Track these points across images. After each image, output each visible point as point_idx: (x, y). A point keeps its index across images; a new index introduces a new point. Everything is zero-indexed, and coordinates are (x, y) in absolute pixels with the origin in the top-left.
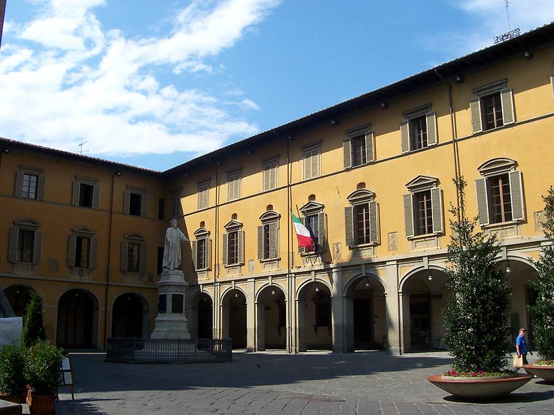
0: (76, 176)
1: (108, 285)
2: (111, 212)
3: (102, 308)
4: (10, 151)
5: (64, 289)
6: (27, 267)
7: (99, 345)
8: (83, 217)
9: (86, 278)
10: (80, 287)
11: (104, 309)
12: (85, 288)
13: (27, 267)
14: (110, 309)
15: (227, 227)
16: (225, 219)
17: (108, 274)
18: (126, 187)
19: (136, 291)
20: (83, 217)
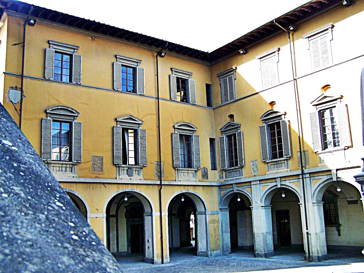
0: (116, 56)
1: (161, 185)
2: (158, 98)
3: (156, 214)
4: (35, 21)
5: (113, 192)
6: (66, 168)
7: (155, 258)
8: (127, 105)
9: (136, 179)
10: (129, 189)
11: (159, 214)
13: (66, 168)
14: (165, 213)
15: (315, 103)
16: (311, 91)
17: (160, 172)
18: (171, 69)
19: (191, 190)
20: (127, 105)
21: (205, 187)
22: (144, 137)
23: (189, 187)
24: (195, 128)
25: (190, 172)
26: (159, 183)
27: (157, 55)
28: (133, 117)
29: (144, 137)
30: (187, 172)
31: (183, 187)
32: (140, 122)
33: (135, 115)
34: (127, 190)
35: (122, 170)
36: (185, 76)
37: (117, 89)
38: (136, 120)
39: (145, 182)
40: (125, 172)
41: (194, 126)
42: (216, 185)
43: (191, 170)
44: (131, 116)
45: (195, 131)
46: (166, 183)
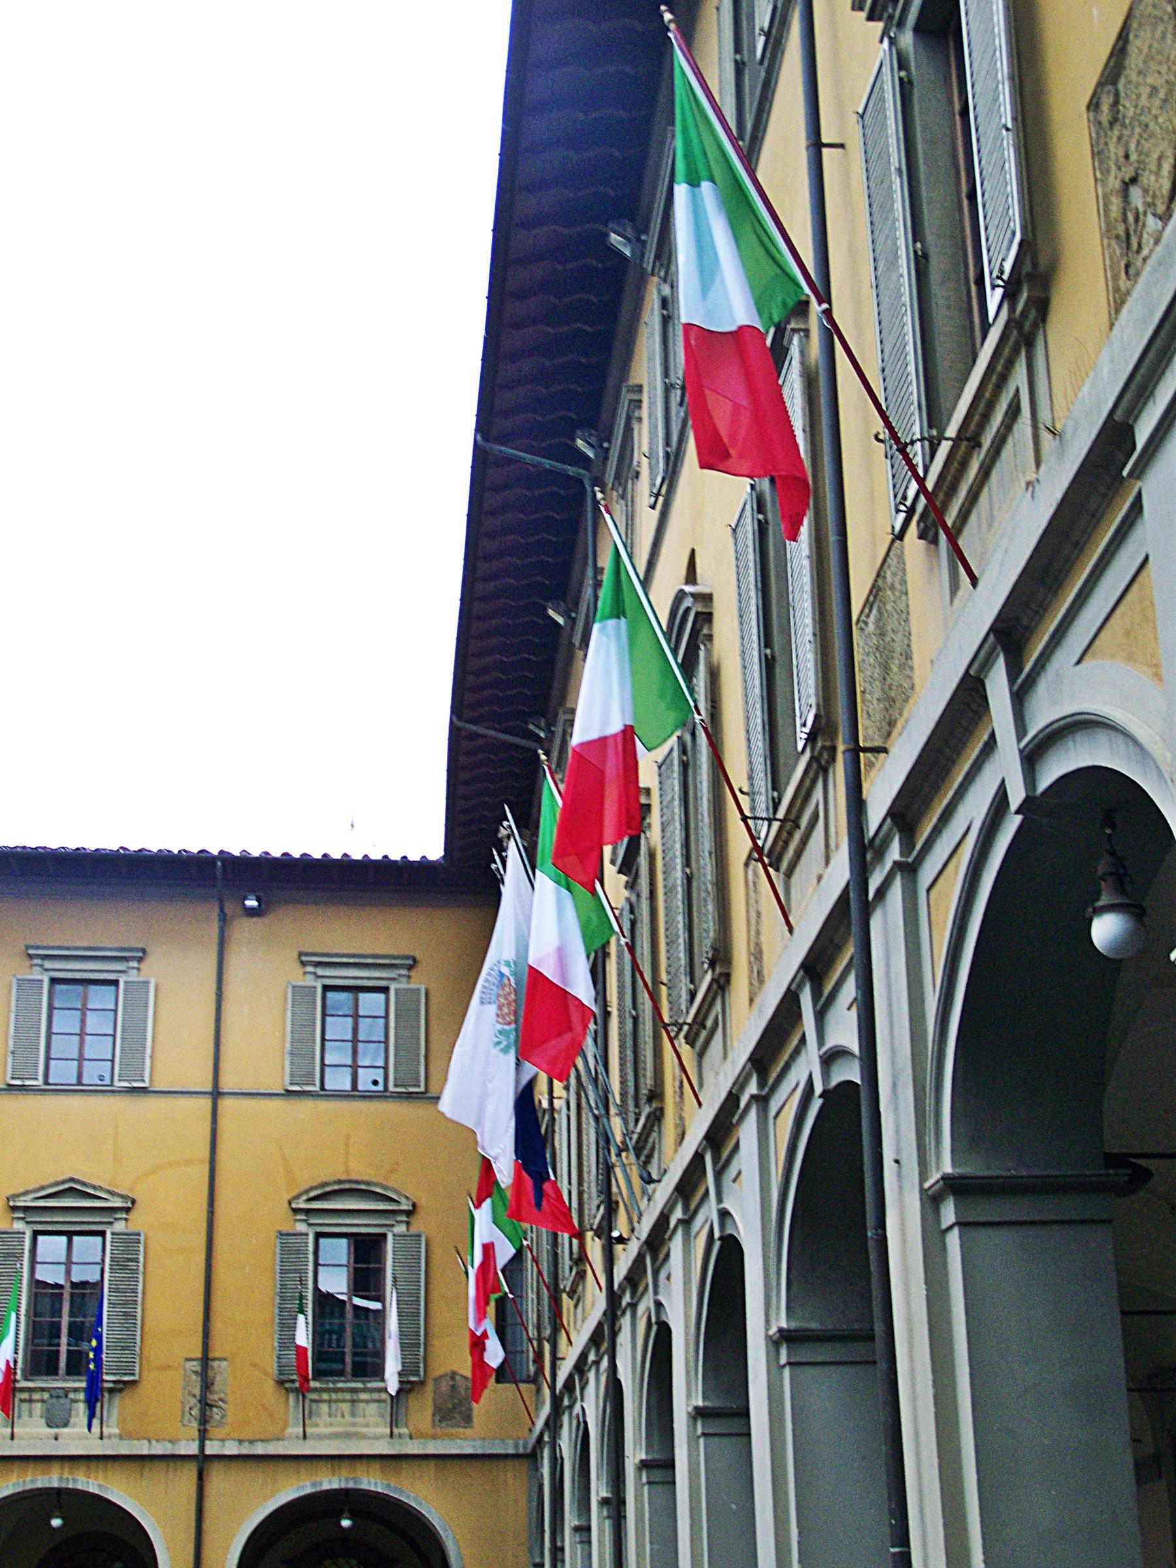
10: (52, 1479)
12: (88, 1482)
18: (301, 954)
19: (372, 1482)
21: (448, 1463)
22: (129, 1260)
23: (360, 1467)
24: (403, 1200)
25: (364, 1396)
26: (192, 1449)
27: (222, 909)
28: (84, 1184)
29: (129, 1260)
30: (348, 1396)
31: (325, 1467)
32: (118, 1203)
33: (94, 1173)
34: (39, 1485)
35: (22, 1401)
36: (377, 974)
37: (18, 1082)
38: (98, 1194)
39: (124, 1449)
40: (38, 1408)
41: (400, 1194)
42: (511, 1451)
43: (372, 1390)
44: (72, 1180)
45: (409, 1213)
46: (231, 1449)
